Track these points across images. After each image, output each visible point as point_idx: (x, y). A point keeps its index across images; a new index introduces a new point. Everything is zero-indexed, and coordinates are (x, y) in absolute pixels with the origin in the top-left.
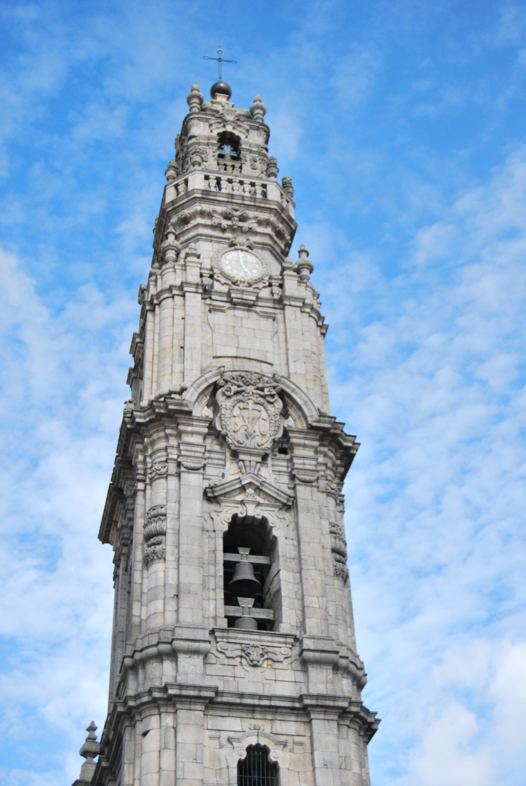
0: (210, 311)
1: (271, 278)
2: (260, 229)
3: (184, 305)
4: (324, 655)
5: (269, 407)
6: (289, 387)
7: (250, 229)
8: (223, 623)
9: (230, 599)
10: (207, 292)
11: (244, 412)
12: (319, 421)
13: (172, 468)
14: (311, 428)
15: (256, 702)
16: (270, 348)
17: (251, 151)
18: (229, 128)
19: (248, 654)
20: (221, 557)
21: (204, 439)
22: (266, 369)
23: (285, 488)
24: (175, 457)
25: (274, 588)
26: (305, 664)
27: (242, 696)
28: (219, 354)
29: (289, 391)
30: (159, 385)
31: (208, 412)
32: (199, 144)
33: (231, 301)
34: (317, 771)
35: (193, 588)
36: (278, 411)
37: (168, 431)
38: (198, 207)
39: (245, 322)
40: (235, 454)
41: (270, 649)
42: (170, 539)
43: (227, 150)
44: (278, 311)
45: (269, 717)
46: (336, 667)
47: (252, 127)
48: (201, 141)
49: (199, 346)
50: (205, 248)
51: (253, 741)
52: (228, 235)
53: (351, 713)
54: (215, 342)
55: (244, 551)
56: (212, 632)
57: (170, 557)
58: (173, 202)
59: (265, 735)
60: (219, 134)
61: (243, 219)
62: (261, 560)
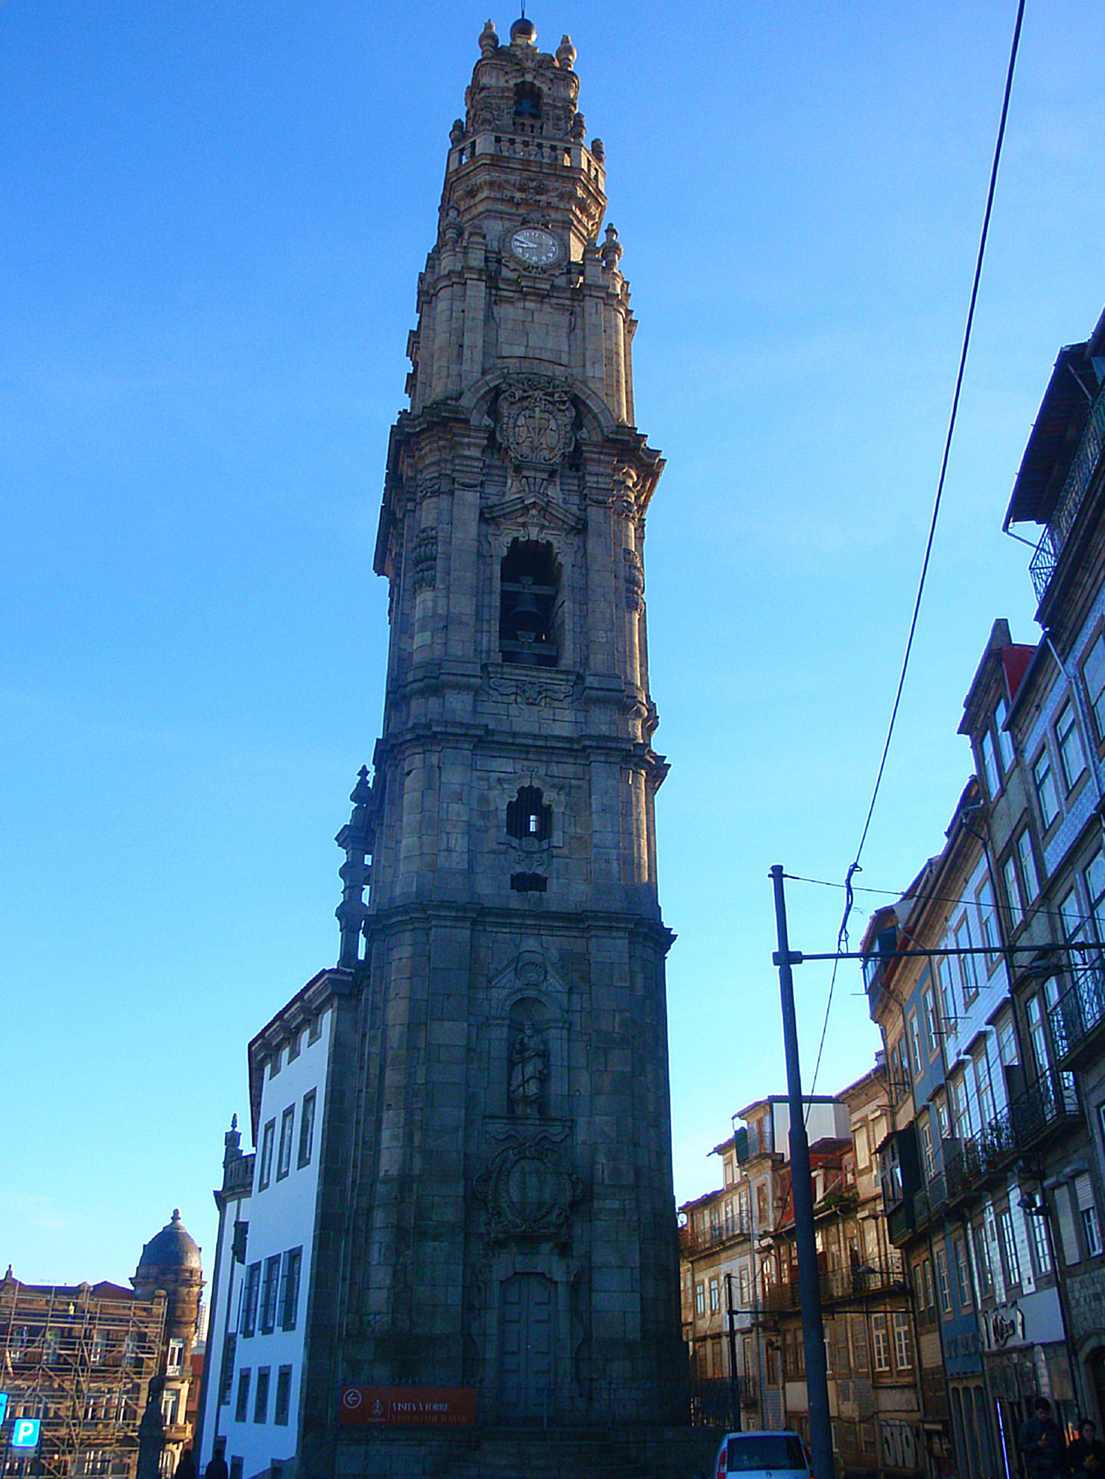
1: (570, 263)
2: (562, 206)
3: (464, 295)
4: (608, 693)
5: (559, 415)
6: (585, 393)
9: (506, 633)
10: (492, 281)
12: (616, 433)
14: (608, 440)
15: (531, 742)
17: (555, 107)
18: (529, 78)
19: (524, 691)
20: (497, 584)
21: (483, 452)
22: (559, 370)
23: (574, 509)
24: (448, 472)
25: (558, 621)
27: (515, 735)
28: (504, 354)
29: (583, 397)
31: (487, 421)
33: (521, 291)
34: (594, 816)
35: (464, 619)
36: (567, 421)
37: (441, 443)
38: (487, 177)
39: (536, 315)
40: (518, 469)
41: (550, 687)
42: (440, 564)
43: (526, 105)
44: (576, 303)
45: (545, 758)
49: (480, 343)
50: (494, 227)
53: (634, 756)
54: (500, 340)
55: (528, 580)
56: (484, 667)
59: (539, 778)
60: (516, 85)
61: (540, 190)
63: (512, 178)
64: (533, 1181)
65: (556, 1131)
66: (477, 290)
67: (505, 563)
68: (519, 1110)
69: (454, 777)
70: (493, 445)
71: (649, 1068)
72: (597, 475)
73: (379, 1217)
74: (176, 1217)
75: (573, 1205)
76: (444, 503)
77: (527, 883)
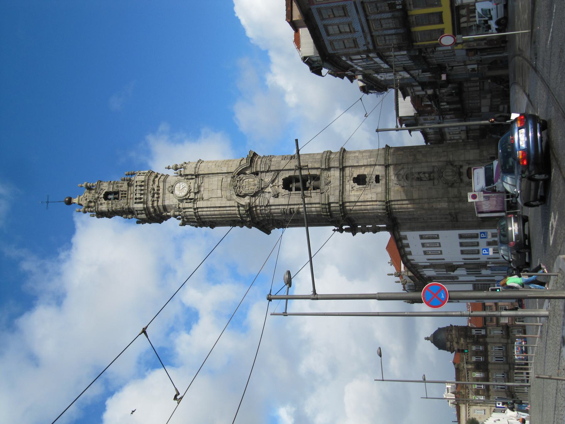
8: (318, 191)
10: (194, 200)
11: (247, 186)
13: (269, 208)
16: (216, 179)
17: (113, 188)
18: (102, 196)
26: (329, 169)
27: (340, 185)
30: (235, 214)
31: (247, 198)
32: (112, 207)
33: (198, 192)
42: (292, 207)
47: (99, 187)
48: (110, 207)
49: (219, 202)
51: (352, 181)
52: (161, 195)
56: (321, 193)
58: (146, 215)
61: (154, 190)
64: (447, 174)
65: (436, 170)
66: (200, 204)
67: (290, 190)
68: (432, 178)
69: (353, 199)
70: (255, 195)
73: (456, 206)
75: (452, 165)
77: (377, 179)
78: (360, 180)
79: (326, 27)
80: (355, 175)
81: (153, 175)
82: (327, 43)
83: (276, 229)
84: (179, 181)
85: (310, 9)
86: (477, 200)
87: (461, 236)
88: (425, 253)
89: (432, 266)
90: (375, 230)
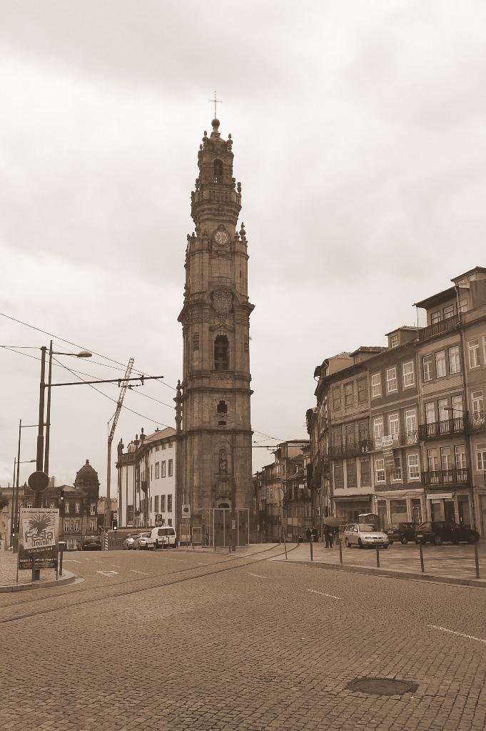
0: (211, 258)
2: (229, 214)
7: (225, 214)
8: (214, 368)
9: (216, 359)
10: (210, 251)
13: (200, 320)
17: (226, 169)
18: (218, 158)
26: (235, 379)
31: (210, 301)
40: (218, 316)
46: (243, 379)
49: (207, 274)
57: (200, 350)
58: (198, 202)
61: (222, 210)
62: (225, 346)
63: (215, 207)
66: (206, 256)
67: (216, 342)
68: (222, 472)
69: (206, 400)
70: (212, 308)
71: (248, 462)
72: (238, 313)
73: (194, 494)
74: (87, 462)
76: (200, 325)
78: (222, 408)
79: (352, 383)
80: (226, 403)
81: (236, 210)
82: (339, 383)
83: (182, 327)
84: (229, 235)
85: (366, 370)
86: (183, 512)
87: (170, 496)
88: (157, 464)
89: (147, 469)
90: (178, 419)
